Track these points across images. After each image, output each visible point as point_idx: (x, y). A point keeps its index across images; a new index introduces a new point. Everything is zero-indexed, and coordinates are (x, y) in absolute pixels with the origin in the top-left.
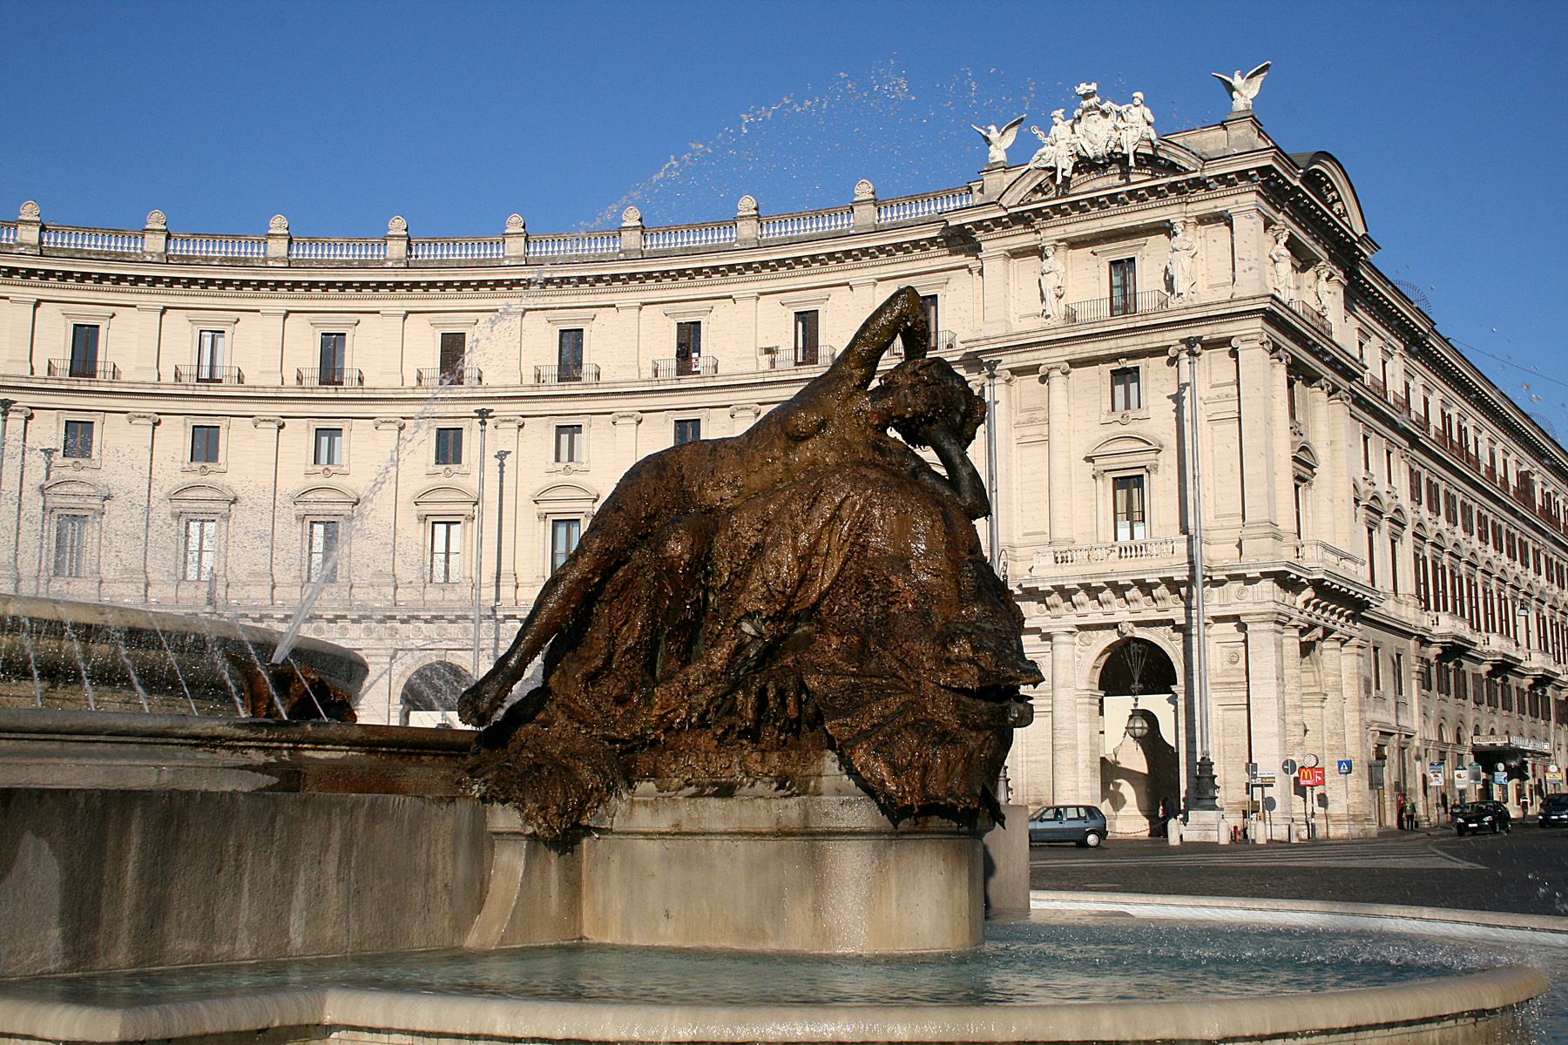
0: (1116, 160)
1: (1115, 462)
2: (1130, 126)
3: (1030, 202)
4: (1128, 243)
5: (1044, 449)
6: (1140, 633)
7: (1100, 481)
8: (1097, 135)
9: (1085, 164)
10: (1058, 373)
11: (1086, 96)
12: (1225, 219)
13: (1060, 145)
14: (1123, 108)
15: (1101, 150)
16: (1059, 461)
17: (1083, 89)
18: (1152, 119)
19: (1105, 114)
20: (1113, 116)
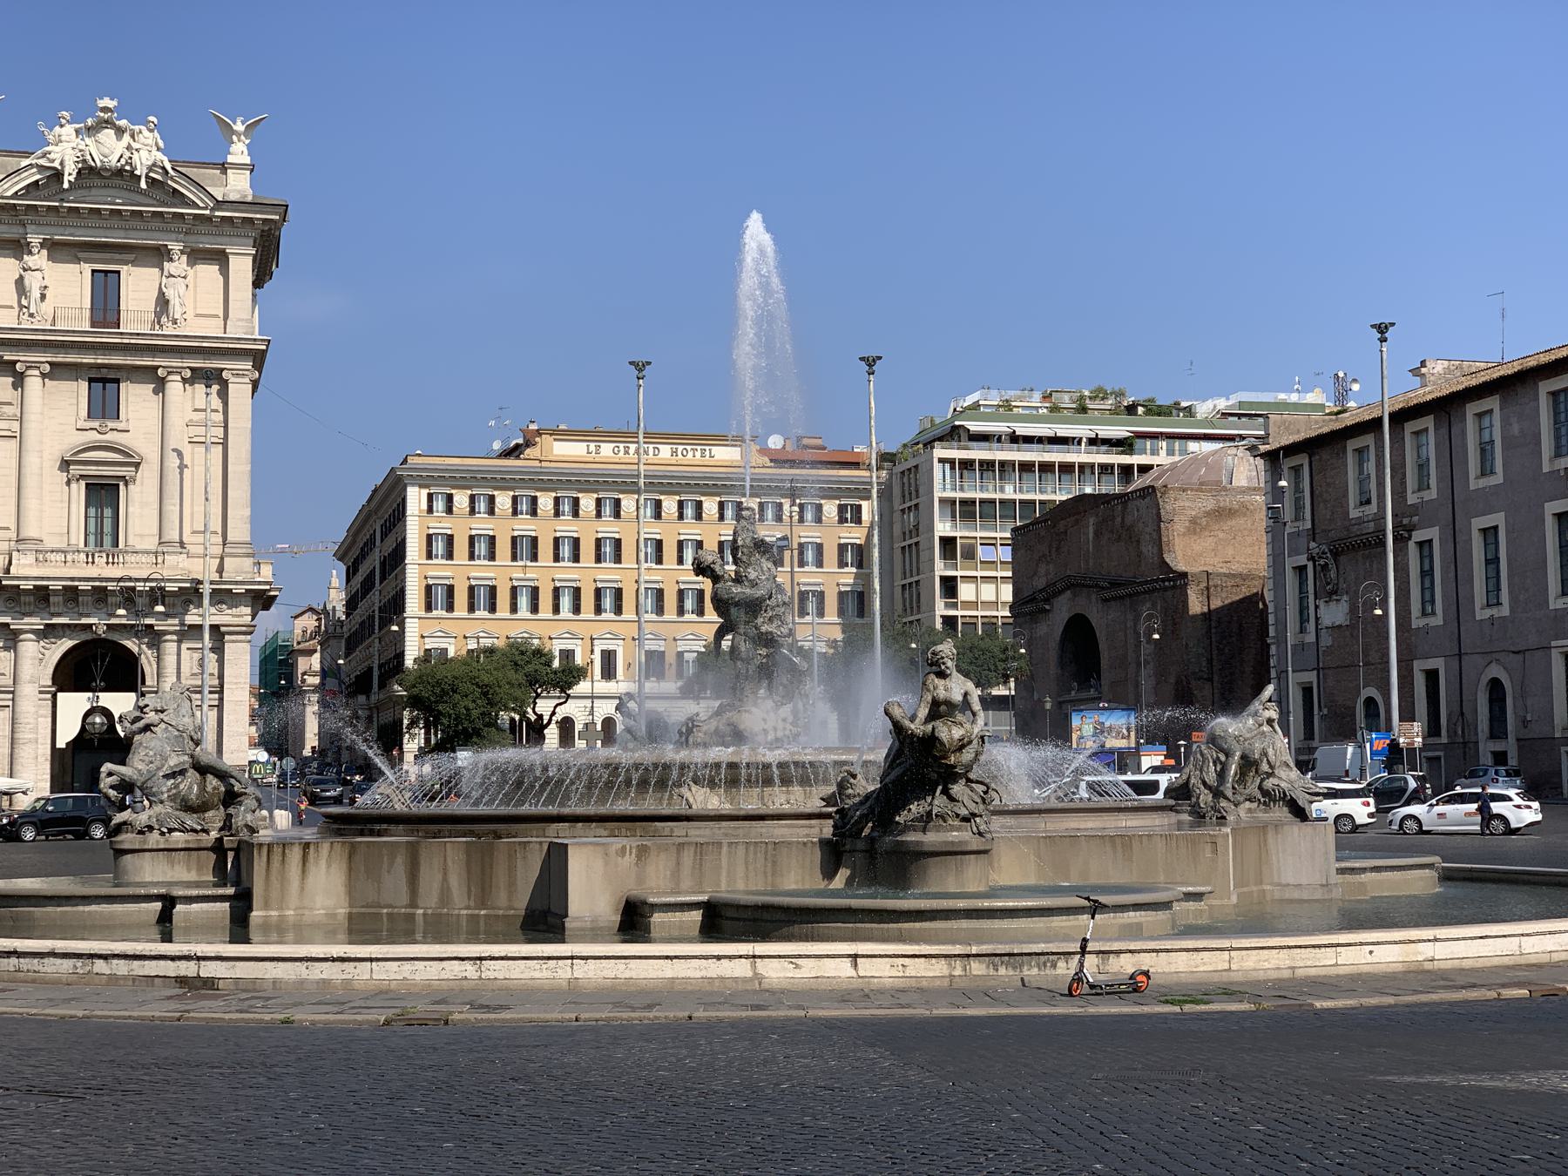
0: (122, 176)
1: (92, 470)
2: (145, 151)
3: (22, 197)
4: (117, 256)
5: (14, 444)
6: (115, 637)
7: (74, 485)
8: (108, 149)
9: (88, 172)
10: (37, 372)
11: (105, 109)
12: (221, 259)
13: (66, 148)
14: (137, 128)
15: (113, 161)
16: (31, 460)
17: (107, 102)
18: (161, 144)
19: (120, 132)
20: (127, 138)
